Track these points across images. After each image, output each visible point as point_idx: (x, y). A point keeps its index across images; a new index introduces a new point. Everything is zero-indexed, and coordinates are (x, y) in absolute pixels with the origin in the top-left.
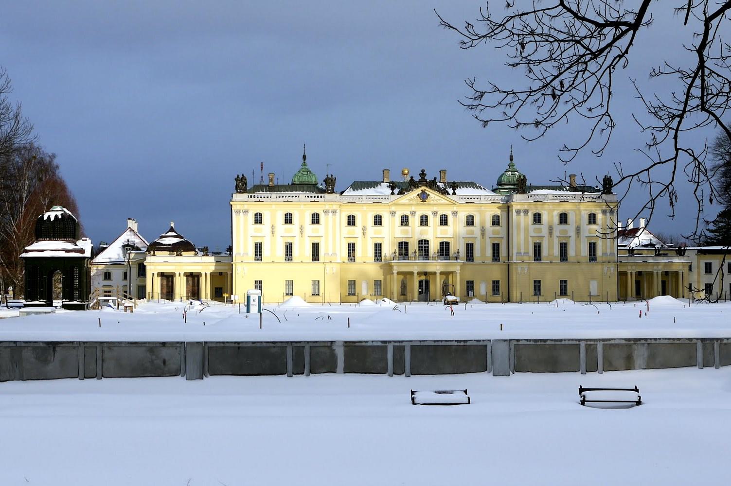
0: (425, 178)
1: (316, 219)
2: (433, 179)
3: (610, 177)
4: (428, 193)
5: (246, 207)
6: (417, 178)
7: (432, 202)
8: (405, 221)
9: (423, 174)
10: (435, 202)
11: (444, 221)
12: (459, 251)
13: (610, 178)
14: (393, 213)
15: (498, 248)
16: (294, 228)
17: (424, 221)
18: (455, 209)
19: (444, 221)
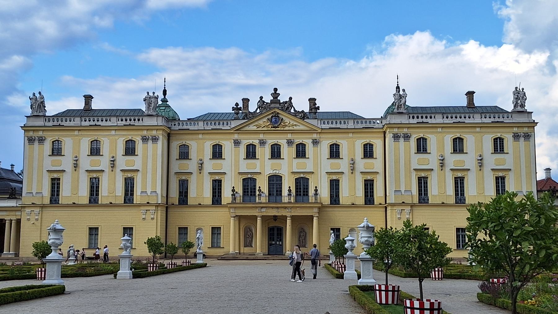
0: (278, 98)
1: (130, 150)
2: (288, 100)
3: (523, 89)
4: (280, 116)
5: (40, 134)
6: (268, 99)
7: (287, 128)
8: (251, 153)
9: (275, 94)
10: (291, 128)
11: (301, 152)
12: (319, 189)
13: (523, 91)
14: (237, 143)
15: (372, 185)
16: (103, 162)
17: (276, 153)
18: (315, 136)
19: (301, 152)
